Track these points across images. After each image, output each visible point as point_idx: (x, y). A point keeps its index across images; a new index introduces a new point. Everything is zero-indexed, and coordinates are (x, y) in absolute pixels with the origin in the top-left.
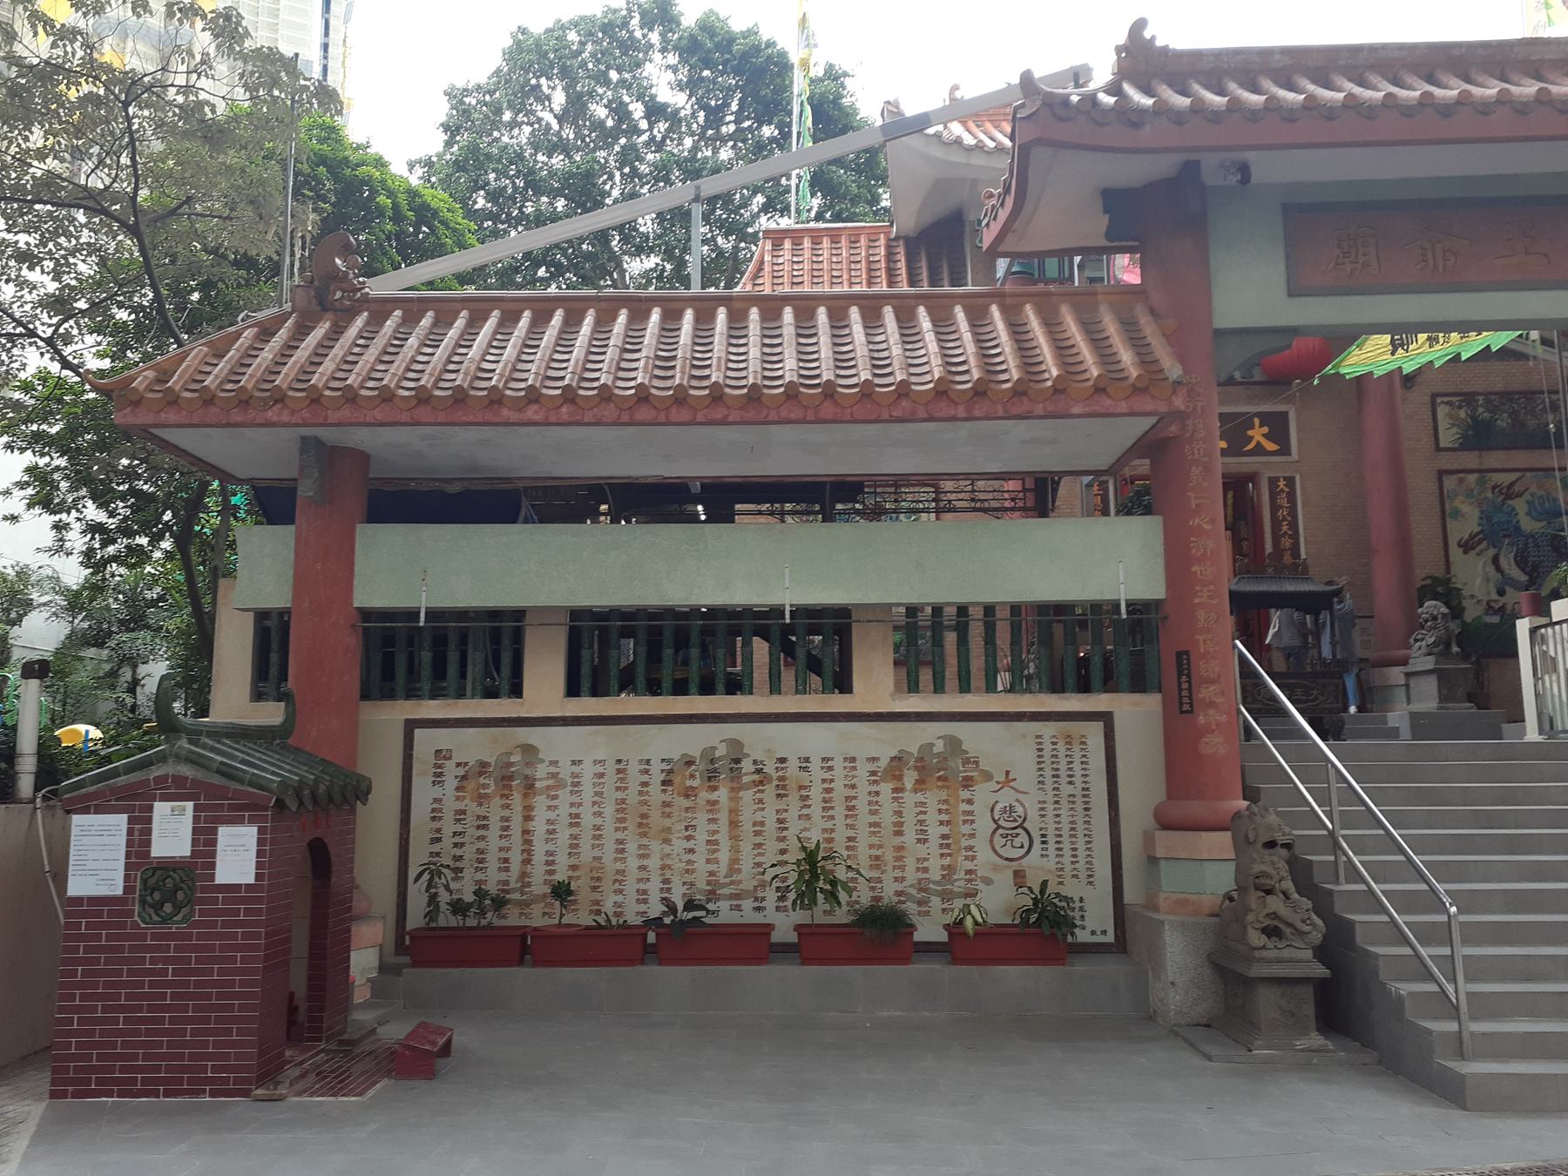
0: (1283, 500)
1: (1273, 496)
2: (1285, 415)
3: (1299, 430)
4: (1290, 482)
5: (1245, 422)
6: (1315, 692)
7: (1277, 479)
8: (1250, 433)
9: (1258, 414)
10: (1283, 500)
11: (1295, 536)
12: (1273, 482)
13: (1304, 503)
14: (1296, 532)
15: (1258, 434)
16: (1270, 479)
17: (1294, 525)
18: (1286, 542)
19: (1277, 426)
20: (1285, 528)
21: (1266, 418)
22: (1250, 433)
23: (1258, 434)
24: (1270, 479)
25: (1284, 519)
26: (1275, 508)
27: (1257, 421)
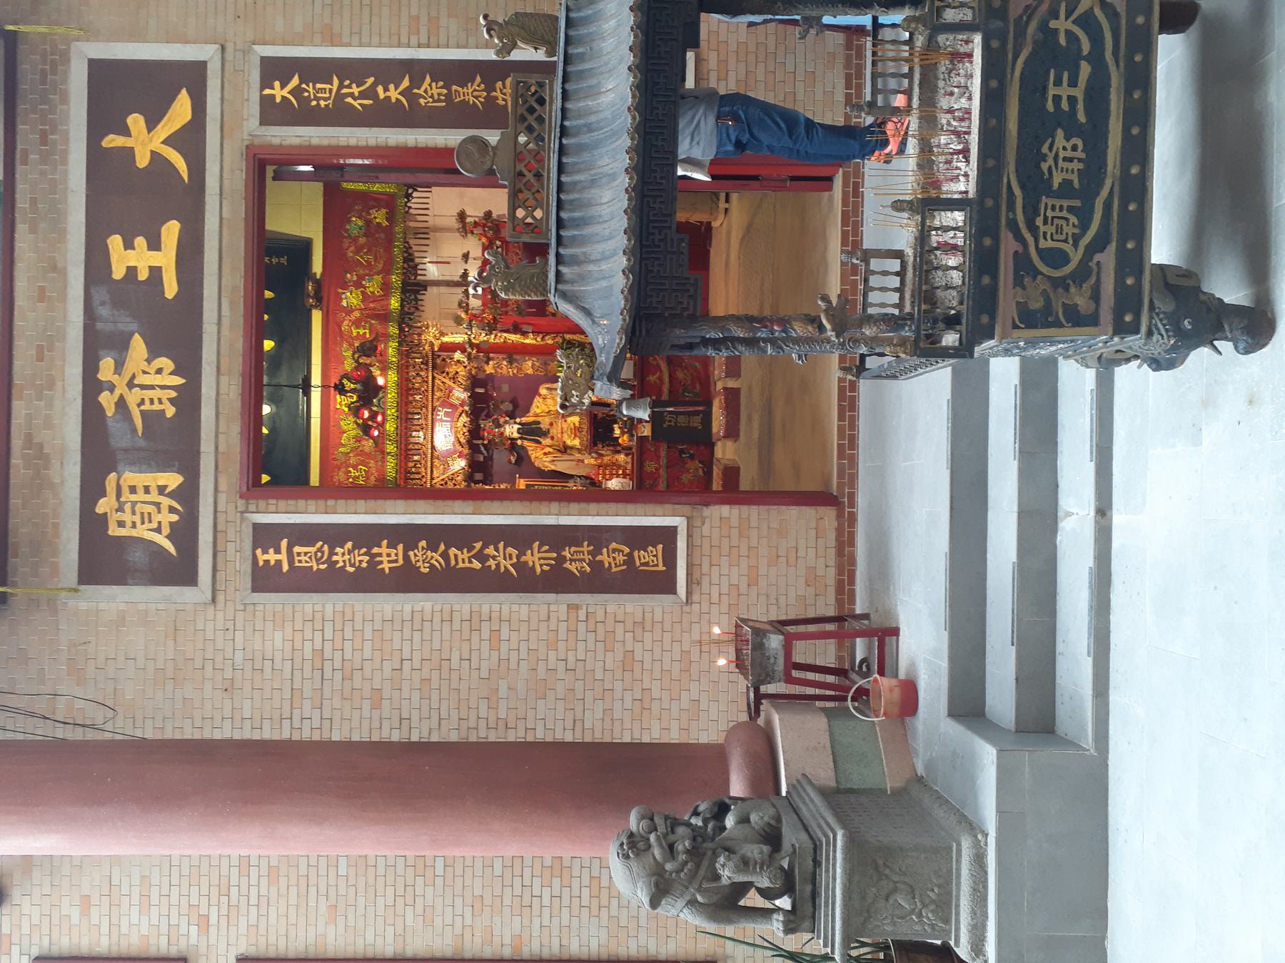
0: (323, 93)
1: (305, 115)
2: (96, 67)
3: (136, 35)
4: (274, 70)
5: (107, 170)
6: (1062, 25)
7: (267, 102)
8: (142, 161)
9: (96, 130)
10: (323, 93)
11: (415, 69)
12: (272, 113)
13: (333, 41)
14: (409, 67)
15: (145, 141)
16: (264, 121)
17: (388, 71)
18: (430, 91)
19: (126, 90)
20: (394, 94)
21: (104, 118)
22: (142, 161)
23: (145, 141)
24: (264, 121)
25: (370, 93)
26: (340, 115)
27: (112, 141)
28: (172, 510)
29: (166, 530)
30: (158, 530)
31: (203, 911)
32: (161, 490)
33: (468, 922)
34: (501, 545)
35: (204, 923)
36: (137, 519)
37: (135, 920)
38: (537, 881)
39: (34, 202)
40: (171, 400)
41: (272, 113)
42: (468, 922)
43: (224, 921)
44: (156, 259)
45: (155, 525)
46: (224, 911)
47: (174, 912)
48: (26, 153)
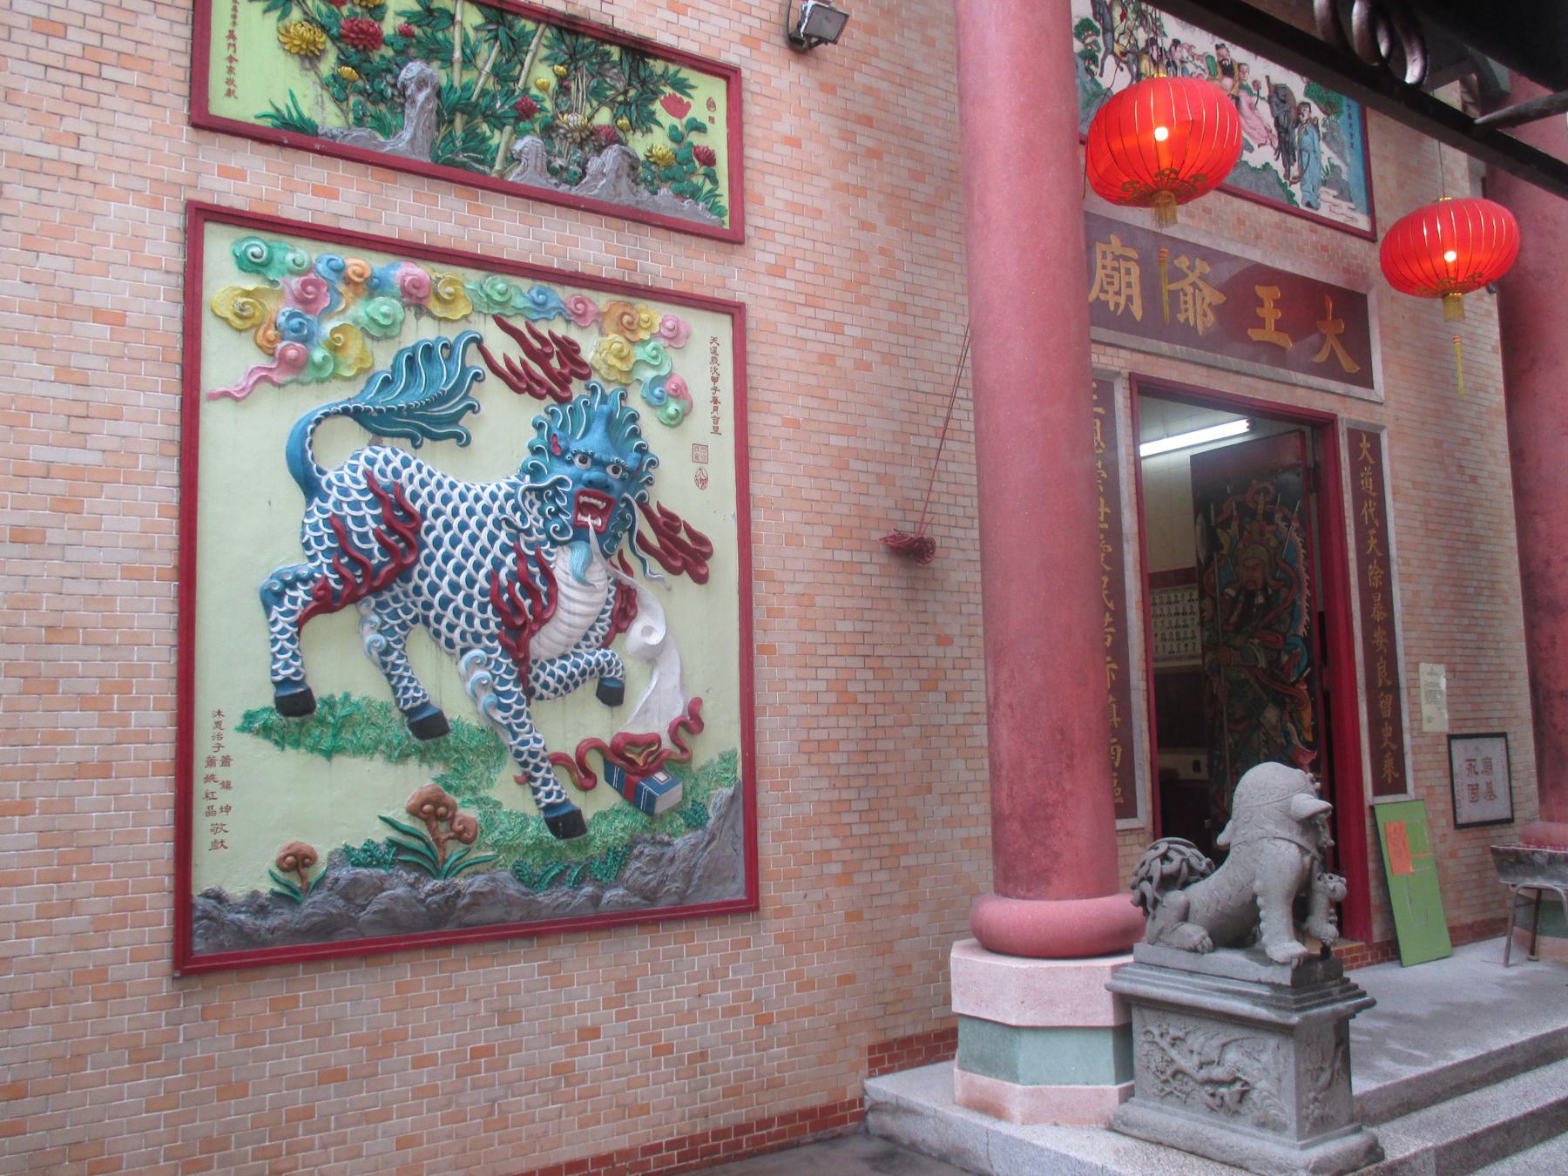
28: (1117, 305)
29: (1103, 297)
30: (1103, 290)
31: (789, 273)
32: (1129, 299)
33: (789, 589)
34: (1112, 630)
35: (777, 271)
36: (1109, 271)
37: (779, 193)
38: (831, 674)
39: (1289, 230)
40: (1187, 320)
41: (1355, 435)
42: (789, 589)
43: (780, 295)
44: (1270, 324)
45: (1106, 287)
46: (790, 297)
47: (788, 240)
48: (1313, 231)
